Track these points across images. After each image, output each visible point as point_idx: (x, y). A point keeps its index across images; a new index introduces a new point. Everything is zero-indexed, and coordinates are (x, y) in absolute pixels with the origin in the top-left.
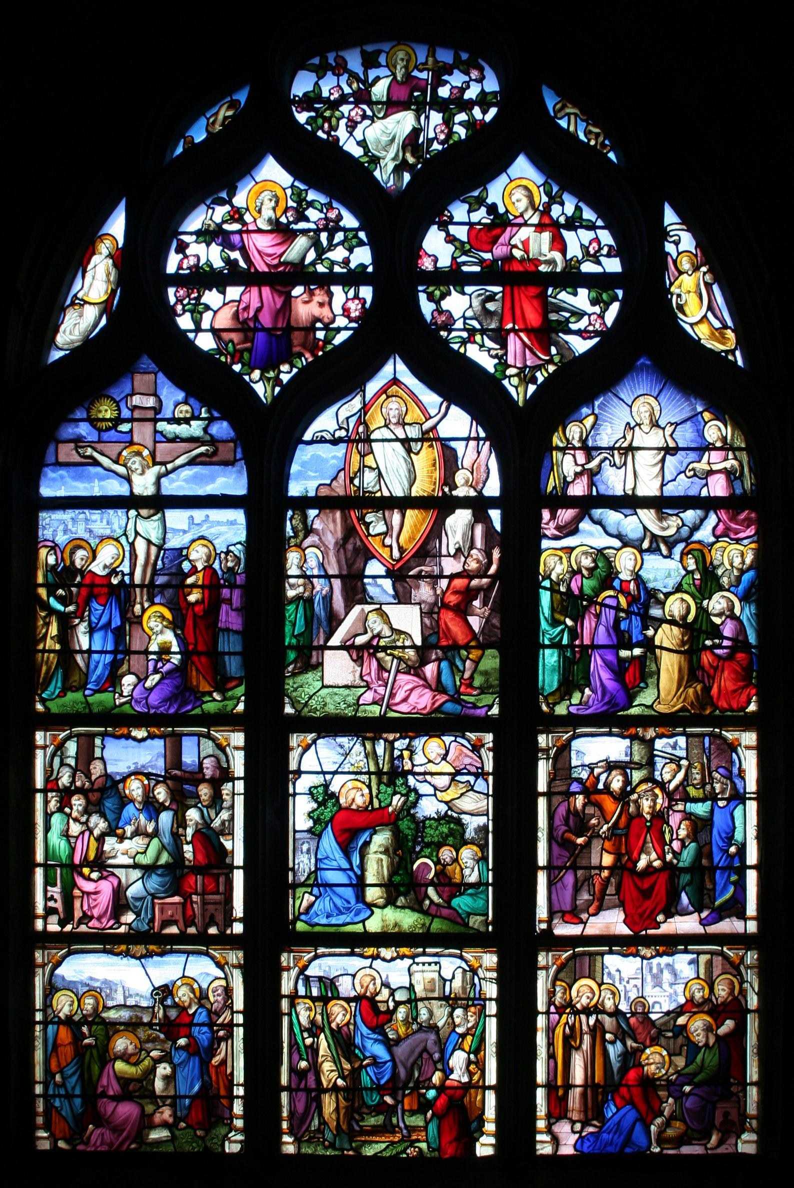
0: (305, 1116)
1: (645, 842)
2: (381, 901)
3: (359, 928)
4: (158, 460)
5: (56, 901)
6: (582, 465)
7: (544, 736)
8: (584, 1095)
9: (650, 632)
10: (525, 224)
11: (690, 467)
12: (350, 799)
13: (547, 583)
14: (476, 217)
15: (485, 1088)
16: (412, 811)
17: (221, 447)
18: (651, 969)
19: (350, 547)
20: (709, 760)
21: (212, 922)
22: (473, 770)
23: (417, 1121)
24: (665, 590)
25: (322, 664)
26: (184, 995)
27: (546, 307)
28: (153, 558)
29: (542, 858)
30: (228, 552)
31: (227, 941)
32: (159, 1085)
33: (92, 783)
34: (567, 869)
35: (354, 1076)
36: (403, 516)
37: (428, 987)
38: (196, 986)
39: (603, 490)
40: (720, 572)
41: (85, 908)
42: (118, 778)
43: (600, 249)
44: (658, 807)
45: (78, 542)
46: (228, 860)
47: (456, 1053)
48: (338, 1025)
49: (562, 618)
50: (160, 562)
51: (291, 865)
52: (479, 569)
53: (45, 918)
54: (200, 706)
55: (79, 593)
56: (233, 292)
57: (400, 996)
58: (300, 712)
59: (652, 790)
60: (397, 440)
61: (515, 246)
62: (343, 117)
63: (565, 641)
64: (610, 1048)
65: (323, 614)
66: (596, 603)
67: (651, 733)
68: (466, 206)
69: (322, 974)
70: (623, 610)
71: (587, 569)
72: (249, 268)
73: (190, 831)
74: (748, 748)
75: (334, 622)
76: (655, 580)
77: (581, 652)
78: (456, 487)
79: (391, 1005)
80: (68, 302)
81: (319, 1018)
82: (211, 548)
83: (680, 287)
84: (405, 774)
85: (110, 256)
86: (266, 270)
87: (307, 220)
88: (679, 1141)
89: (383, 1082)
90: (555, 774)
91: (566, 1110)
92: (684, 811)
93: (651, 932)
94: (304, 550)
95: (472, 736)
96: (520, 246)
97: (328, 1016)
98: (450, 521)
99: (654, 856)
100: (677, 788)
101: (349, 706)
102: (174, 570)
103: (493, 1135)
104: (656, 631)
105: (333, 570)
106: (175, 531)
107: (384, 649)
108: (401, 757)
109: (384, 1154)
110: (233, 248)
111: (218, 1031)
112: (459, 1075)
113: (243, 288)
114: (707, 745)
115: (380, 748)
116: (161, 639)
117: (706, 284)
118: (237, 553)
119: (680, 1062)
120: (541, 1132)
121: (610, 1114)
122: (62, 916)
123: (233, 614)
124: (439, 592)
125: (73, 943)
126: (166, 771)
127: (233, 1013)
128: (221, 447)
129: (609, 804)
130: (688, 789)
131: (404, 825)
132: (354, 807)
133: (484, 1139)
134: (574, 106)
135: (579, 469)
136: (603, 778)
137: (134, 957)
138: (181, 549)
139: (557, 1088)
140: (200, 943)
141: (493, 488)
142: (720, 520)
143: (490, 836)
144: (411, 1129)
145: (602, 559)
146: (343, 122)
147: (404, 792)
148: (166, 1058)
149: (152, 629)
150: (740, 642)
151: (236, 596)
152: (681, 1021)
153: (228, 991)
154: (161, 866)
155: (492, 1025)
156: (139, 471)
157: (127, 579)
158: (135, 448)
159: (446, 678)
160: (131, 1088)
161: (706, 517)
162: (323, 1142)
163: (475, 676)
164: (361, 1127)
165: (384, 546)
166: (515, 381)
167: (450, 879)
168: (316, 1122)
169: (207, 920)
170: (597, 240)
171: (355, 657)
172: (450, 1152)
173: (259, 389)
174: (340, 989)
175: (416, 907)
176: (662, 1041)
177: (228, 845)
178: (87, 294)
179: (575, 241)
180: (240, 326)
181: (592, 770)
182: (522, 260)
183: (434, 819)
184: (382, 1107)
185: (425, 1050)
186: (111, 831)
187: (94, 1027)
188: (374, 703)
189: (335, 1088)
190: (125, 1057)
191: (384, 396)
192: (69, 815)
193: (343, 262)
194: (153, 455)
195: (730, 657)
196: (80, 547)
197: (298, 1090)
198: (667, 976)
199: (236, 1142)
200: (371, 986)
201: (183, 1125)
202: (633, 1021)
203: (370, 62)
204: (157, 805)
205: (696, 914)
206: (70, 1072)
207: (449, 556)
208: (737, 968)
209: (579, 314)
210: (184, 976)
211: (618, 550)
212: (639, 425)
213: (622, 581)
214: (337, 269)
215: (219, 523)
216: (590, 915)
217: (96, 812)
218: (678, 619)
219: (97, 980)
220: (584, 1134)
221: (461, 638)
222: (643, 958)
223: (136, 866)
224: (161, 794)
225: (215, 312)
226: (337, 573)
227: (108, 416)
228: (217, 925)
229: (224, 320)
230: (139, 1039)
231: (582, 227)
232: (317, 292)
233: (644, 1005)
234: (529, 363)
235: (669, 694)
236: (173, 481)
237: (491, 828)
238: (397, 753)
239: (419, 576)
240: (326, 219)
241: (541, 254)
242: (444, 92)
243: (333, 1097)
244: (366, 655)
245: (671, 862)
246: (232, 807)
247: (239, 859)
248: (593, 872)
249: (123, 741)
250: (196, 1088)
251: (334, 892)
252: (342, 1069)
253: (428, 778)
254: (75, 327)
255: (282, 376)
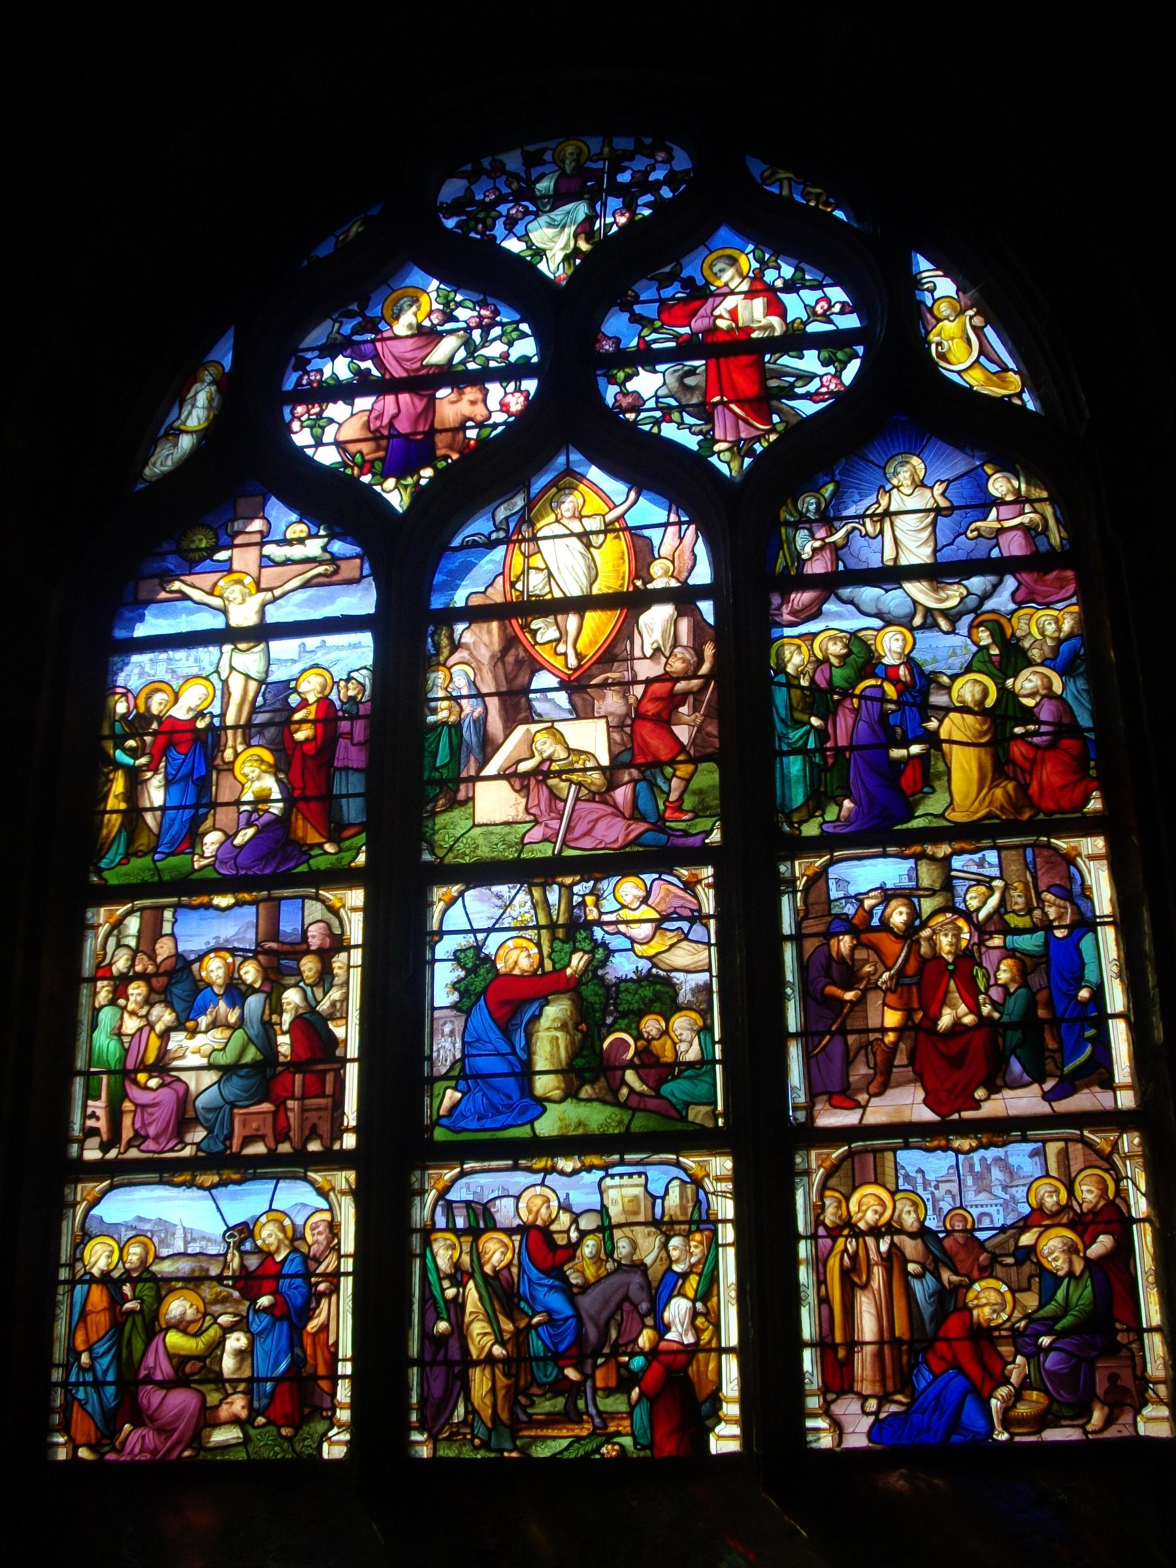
0: (446, 1404)
1: (947, 991)
2: (557, 1094)
3: (523, 1132)
4: (263, 586)
5: (98, 1118)
6: (823, 539)
7: (789, 864)
8: (879, 1357)
9: (933, 724)
10: (732, 293)
11: (973, 526)
12: (511, 962)
13: (782, 678)
14: (667, 293)
15: (721, 1351)
16: (600, 972)
17: (343, 564)
18: (972, 1166)
19: (510, 659)
20: (1035, 878)
21: (314, 1134)
22: (687, 913)
23: (616, 1404)
24: (949, 672)
25: (473, 799)
26: (270, 1235)
27: (763, 374)
28: (251, 694)
29: (793, 1022)
30: (349, 679)
31: (334, 1160)
32: (228, 1364)
33: (158, 966)
34: (833, 1034)
35: (520, 1337)
36: (582, 618)
37: (629, 1207)
38: (287, 1222)
39: (853, 565)
40: (1026, 644)
41: (138, 1125)
42: (192, 957)
43: (830, 306)
44: (964, 944)
45: (157, 685)
46: (339, 1052)
47: (673, 1301)
48: (494, 1267)
49: (805, 718)
50: (260, 699)
51: (427, 1053)
52: (686, 670)
53: (81, 1143)
54: (307, 861)
55: (154, 743)
56: (364, 403)
57: (586, 1223)
58: (442, 859)
59: (952, 922)
60: (572, 534)
61: (721, 317)
62: (501, 215)
63: (811, 745)
64: (917, 1285)
65: (474, 739)
66: (853, 696)
67: (943, 850)
68: (656, 284)
69: (470, 1197)
70: (891, 701)
71: (837, 656)
73: (287, 1018)
74: (1092, 858)
75: (488, 747)
76: (935, 661)
77: (835, 757)
78: (652, 580)
79: (574, 1235)
80: (162, 432)
81: (466, 1259)
82: (328, 676)
83: (939, 334)
84: (589, 925)
85: (214, 382)
86: (404, 374)
87: (456, 320)
88: (1042, 1421)
89: (562, 1347)
90: (807, 911)
91: (852, 1380)
92: (1004, 947)
93: (967, 1114)
94: (449, 669)
95: (684, 872)
96: (726, 316)
97: (477, 1255)
98: (645, 619)
99: (963, 1008)
100: (990, 917)
101: (510, 846)
102: (278, 706)
103: (736, 1422)
104: (941, 722)
105: (487, 687)
106: (280, 661)
107: (559, 774)
108: (583, 904)
109: (566, 1455)
110: (363, 358)
111: (318, 1283)
112: (679, 1333)
114: (1030, 858)
115: (553, 896)
116: (257, 786)
117: (974, 328)
118: (361, 679)
119: (1031, 1300)
120: (814, 1415)
121: (923, 1384)
122: (105, 1137)
123: (354, 749)
124: (632, 700)
125: (118, 1174)
126: (258, 944)
127: (340, 1257)
128: (343, 564)
129: (889, 945)
130: (1007, 917)
131: (588, 991)
132: (517, 972)
133: (722, 1429)
134: (787, 170)
135: (817, 544)
136: (878, 911)
137: (201, 1187)
138: (289, 681)
139: (835, 1347)
140: (297, 1165)
141: (702, 575)
142: (1020, 584)
143: (715, 996)
144: (606, 1417)
145: (857, 643)
146: (500, 223)
147: (588, 948)
148: (241, 1324)
149: (246, 776)
150: (1065, 727)
151: (360, 730)
152: (1026, 1239)
153: (333, 1228)
154: (246, 1065)
155: (728, 1261)
156: (240, 600)
157: (216, 722)
158: (235, 576)
159: (645, 804)
160: (188, 1369)
161: (1000, 582)
162: (472, 1440)
163: (686, 797)
164: (530, 1416)
165: (557, 654)
166: (726, 456)
167: (657, 1058)
168: (461, 1410)
169: (307, 1132)
170: (826, 298)
171: (517, 787)
172: (668, 1448)
174: (497, 1217)
175: (609, 1098)
176: (999, 1270)
177: (339, 1032)
178: (184, 423)
179: (794, 305)
181: (861, 902)
182: (730, 330)
183: (631, 979)
184: (560, 1387)
185: (626, 1298)
186: (179, 1026)
187: (140, 1286)
188: (545, 839)
189: (490, 1360)
190: (181, 1326)
191: (554, 490)
192: (124, 1008)
194: (257, 583)
195: (1052, 746)
196: (158, 690)
197: (434, 1363)
198: (996, 1174)
199: (339, 1443)
200: (543, 1210)
201: (261, 1420)
202: (948, 1243)
203: (532, 160)
204: (243, 988)
205: (1036, 1086)
206: (101, 1350)
207: (645, 657)
208: (1108, 1158)
209: (809, 377)
210: (270, 1210)
211: (879, 630)
212: (898, 487)
213: (886, 666)
214: (492, 364)
215: (339, 648)
216: (871, 1096)
217: (160, 1002)
218: (971, 705)
219: (149, 1221)
220: (882, 1416)
221: (664, 755)
222: (958, 1152)
223: (210, 1067)
224: (250, 973)
225: (340, 425)
226: (493, 690)
227: (203, 545)
228: (320, 1137)
229: (352, 431)
230: (203, 1299)
231: (804, 287)
233: (965, 1219)
234: (743, 435)
235: (966, 796)
236: (281, 606)
237: (715, 987)
238: (576, 900)
239: (605, 685)
241: (753, 321)
242: (625, 177)
243: (487, 1372)
244: (533, 782)
245: (989, 1017)
246: (347, 983)
247: (353, 1050)
248: (872, 1037)
249: (202, 911)
250: (283, 1366)
251: (490, 1086)
252: (501, 1331)
253: (622, 928)
254: (167, 458)
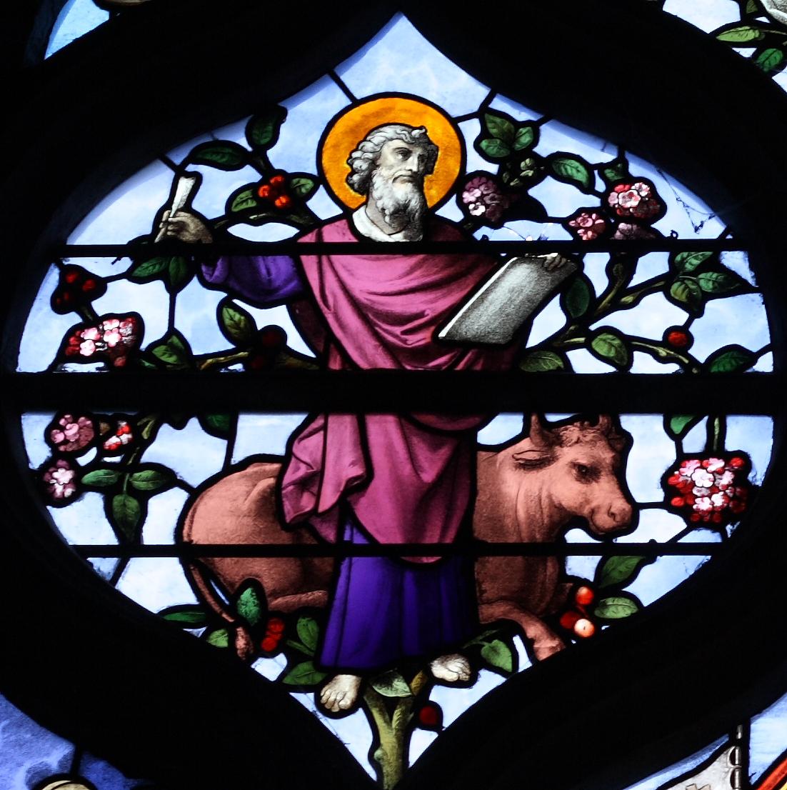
56: (263, 432)
72: (322, 357)
86: (384, 362)
87: (537, 213)
113: (295, 420)
173: (354, 734)
180: (284, 538)
193: (665, 343)
214: (643, 364)
225: (195, 494)
232: (573, 432)
240: (605, 210)
255: (437, 694)
